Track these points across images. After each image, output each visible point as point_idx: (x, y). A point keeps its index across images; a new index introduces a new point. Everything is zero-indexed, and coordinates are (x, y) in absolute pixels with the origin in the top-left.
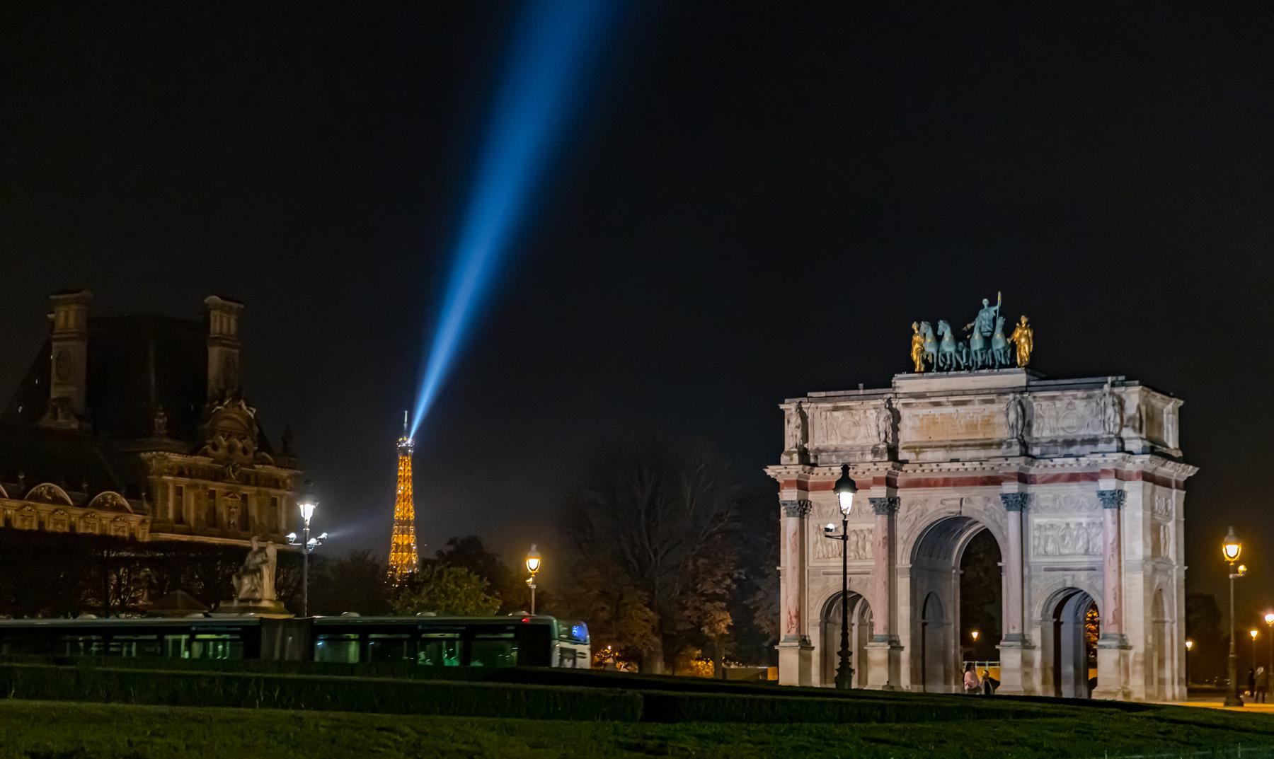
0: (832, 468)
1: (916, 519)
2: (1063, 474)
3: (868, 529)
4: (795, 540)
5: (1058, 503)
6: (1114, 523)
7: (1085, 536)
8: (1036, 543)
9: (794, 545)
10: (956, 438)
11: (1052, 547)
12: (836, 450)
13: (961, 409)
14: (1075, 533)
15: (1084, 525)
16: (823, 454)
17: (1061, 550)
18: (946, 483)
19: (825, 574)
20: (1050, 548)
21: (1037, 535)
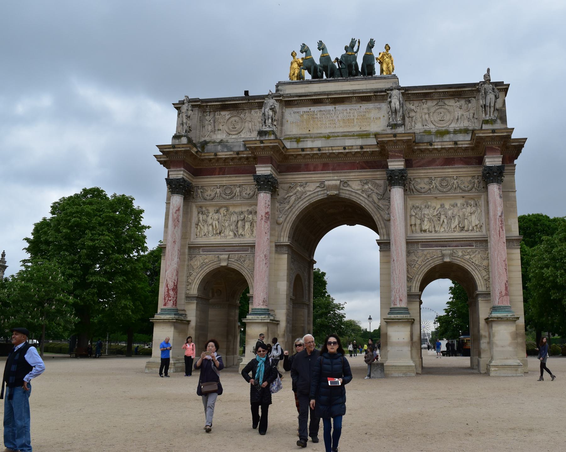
1: (295, 200)
2: (438, 159)
3: (248, 210)
5: (433, 184)
6: (501, 197)
7: (461, 214)
8: (413, 223)
10: (333, 131)
12: (221, 142)
13: (340, 107)
14: (450, 213)
15: (459, 205)
16: (208, 144)
17: (437, 229)
18: (325, 167)
20: (426, 226)
21: (414, 214)
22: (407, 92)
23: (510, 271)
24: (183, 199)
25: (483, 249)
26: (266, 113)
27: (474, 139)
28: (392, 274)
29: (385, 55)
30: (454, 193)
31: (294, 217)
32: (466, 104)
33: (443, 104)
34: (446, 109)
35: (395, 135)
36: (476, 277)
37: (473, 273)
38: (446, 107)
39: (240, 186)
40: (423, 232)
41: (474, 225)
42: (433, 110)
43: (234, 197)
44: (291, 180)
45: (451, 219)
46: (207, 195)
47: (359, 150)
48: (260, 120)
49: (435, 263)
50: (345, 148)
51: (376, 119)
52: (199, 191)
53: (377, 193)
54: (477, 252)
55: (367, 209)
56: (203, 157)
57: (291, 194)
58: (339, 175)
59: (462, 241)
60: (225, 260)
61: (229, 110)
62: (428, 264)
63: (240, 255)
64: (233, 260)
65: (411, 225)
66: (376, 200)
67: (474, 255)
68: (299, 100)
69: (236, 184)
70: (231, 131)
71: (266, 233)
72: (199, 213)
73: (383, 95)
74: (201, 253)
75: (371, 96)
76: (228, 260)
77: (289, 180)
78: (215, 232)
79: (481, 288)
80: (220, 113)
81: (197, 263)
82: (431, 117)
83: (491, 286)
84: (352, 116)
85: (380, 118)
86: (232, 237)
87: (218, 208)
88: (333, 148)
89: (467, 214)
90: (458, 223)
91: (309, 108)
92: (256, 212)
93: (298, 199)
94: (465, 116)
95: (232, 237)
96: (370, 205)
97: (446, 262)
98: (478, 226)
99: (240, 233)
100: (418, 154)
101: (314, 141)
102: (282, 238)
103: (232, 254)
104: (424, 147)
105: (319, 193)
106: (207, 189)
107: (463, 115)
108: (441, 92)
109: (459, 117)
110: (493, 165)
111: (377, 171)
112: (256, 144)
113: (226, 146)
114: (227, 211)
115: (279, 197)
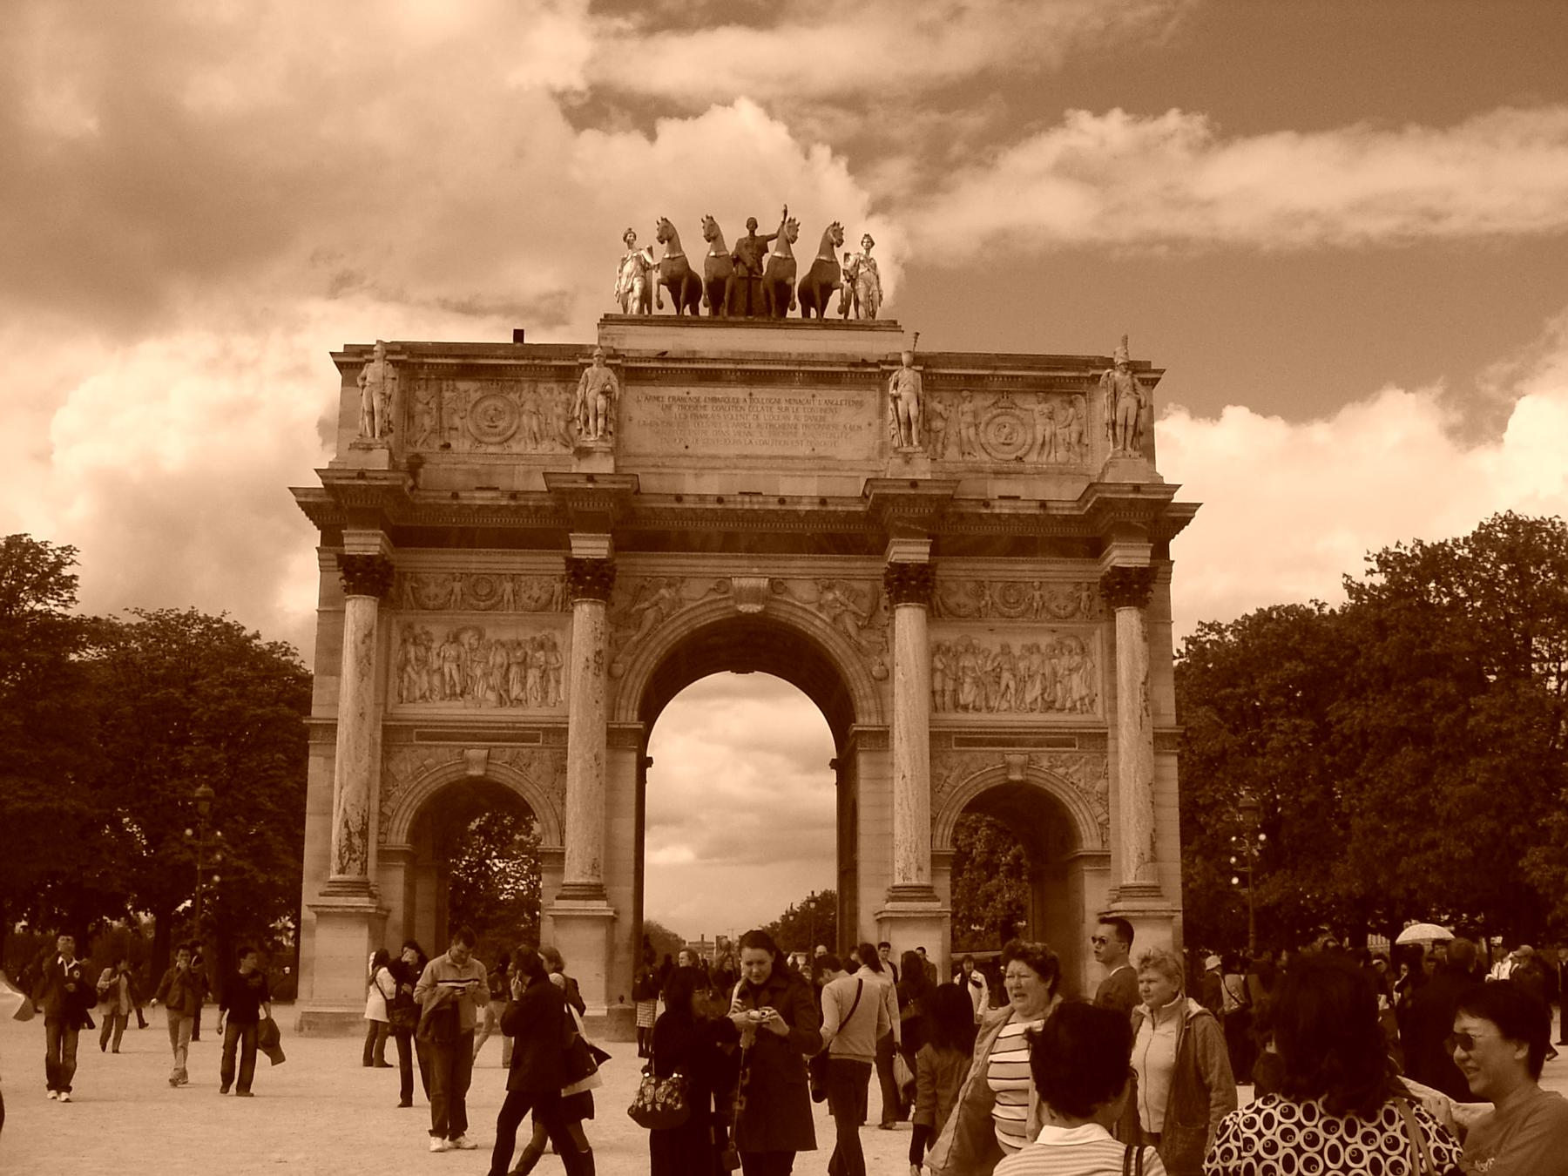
0: (462, 494)
1: (656, 621)
3: (533, 639)
4: (369, 649)
5: (987, 598)
6: (1145, 639)
7: (1048, 671)
8: (938, 686)
9: (365, 661)
11: (973, 693)
13: (762, 393)
15: (1043, 647)
16: (425, 466)
17: (992, 704)
18: (729, 544)
19: (421, 737)
20: (968, 695)
21: (940, 666)
22: (928, 370)
23: (1159, 806)
24: (376, 604)
25: (1098, 755)
26: (590, 402)
27: (1087, 501)
28: (896, 806)
29: (862, 262)
30: (1033, 621)
31: (652, 663)
32: (1064, 408)
33: (1007, 405)
34: (1018, 417)
35: (914, 484)
36: (1079, 818)
37: (1073, 809)
38: (1017, 412)
39: (513, 578)
40: (959, 710)
41: (1076, 696)
42: (985, 417)
43: (498, 603)
44: (645, 569)
45: (1025, 682)
46: (428, 597)
47: (816, 508)
48: (560, 410)
49: (989, 781)
50: (782, 501)
51: (852, 428)
52: (407, 586)
53: (854, 613)
54: (1083, 760)
55: (831, 650)
56: (423, 502)
57: (646, 605)
58: (764, 563)
59: (1051, 733)
60: (478, 763)
61: (480, 380)
62: (971, 784)
63: (516, 751)
64: (499, 762)
65: (933, 693)
66: (852, 630)
67: (1077, 767)
68: (662, 369)
69: (503, 572)
70: (487, 434)
71: (597, 702)
72: (404, 641)
73: (870, 373)
74: (415, 742)
75: (842, 373)
76: (488, 763)
77: (639, 568)
78: (448, 692)
79: (1089, 843)
80: (454, 385)
81: (406, 767)
82: (981, 434)
83: (1111, 838)
84: (792, 418)
85: (860, 427)
86: (495, 704)
87: (455, 630)
88: (755, 499)
89: (1061, 671)
90: (1040, 692)
91: (686, 389)
92: (555, 645)
93: (661, 619)
94: (1060, 438)
95: (495, 704)
96: (839, 640)
97: (1012, 782)
98: (1087, 701)
99: (513, 695)
100: (953, 523)
101: (702, 475)
102: (623, 714)
103: (495, 747)
104: (970, 510)
105: (714, 606)
106: (426, 580)
107: (1055, 435)
108: (1008, 377)
109: (1047, 439)
110: (1133, 566)
111: (857, 560)
112: (575, 482)
113: (477, 473)
114: (479, 639)
115: (614, 611)
